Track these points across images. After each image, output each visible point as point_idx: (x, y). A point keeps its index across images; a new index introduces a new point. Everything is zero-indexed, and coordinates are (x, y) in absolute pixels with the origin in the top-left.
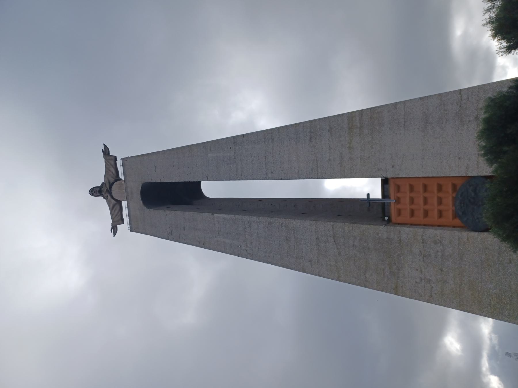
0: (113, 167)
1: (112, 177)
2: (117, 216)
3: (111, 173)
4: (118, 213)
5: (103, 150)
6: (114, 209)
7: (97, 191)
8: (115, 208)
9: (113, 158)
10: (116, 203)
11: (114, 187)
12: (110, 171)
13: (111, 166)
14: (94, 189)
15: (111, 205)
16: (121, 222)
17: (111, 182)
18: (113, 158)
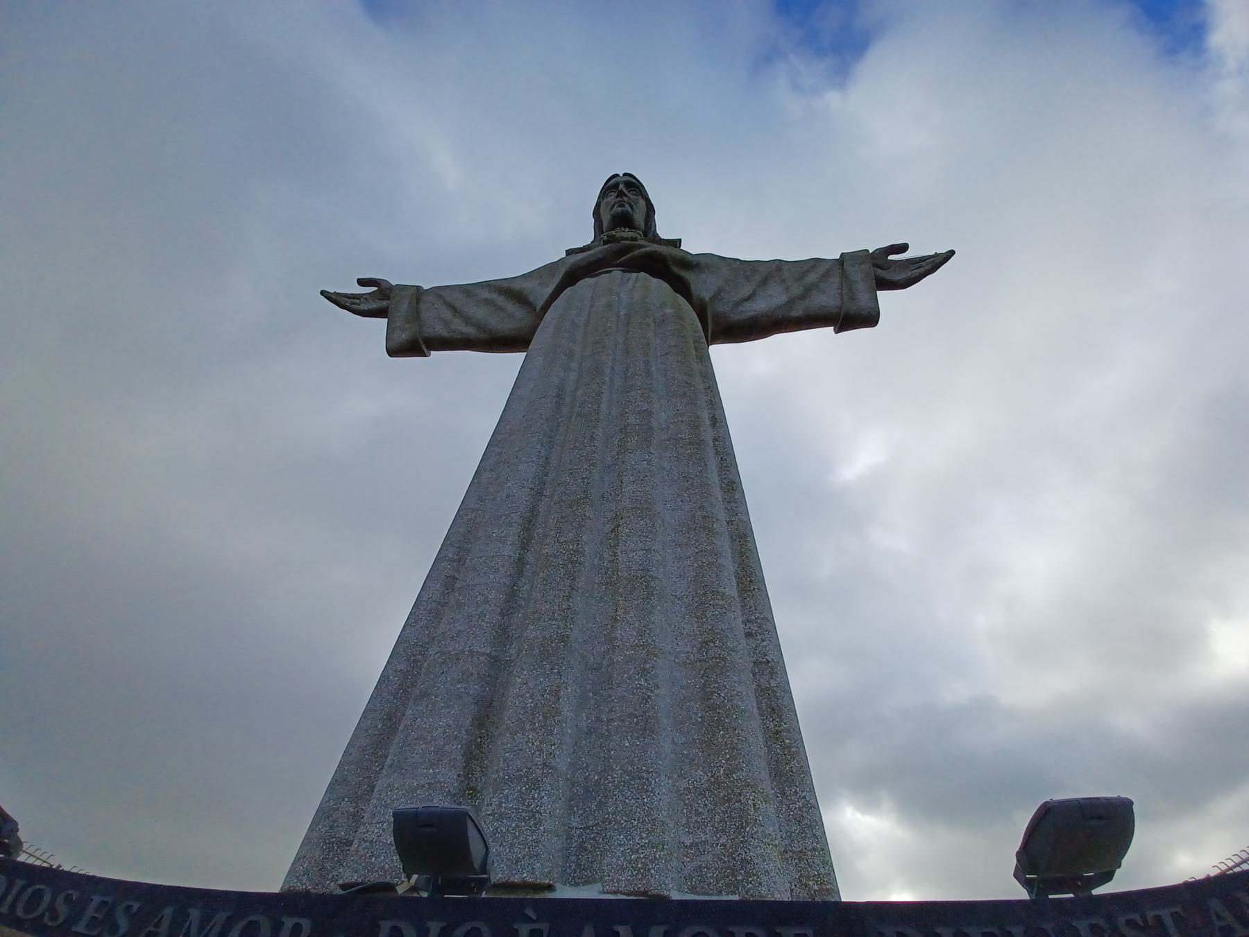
0: (791, 303)
1: (717, 296)
2: (446, 314)
3: (746, 290)
4: (467, 320)
5: (903, 248)
6: (501, 300)
7: (628, 208)
8: (511, 307)
9: (863, 300)
10: (538, 309)
11: (659, 287)
12: (764, 282)
13: (797, 290)
14: (642, 202)
15: (527, 285)
16: (402, 336)
17: (689, 276)
18: (863, 300)
